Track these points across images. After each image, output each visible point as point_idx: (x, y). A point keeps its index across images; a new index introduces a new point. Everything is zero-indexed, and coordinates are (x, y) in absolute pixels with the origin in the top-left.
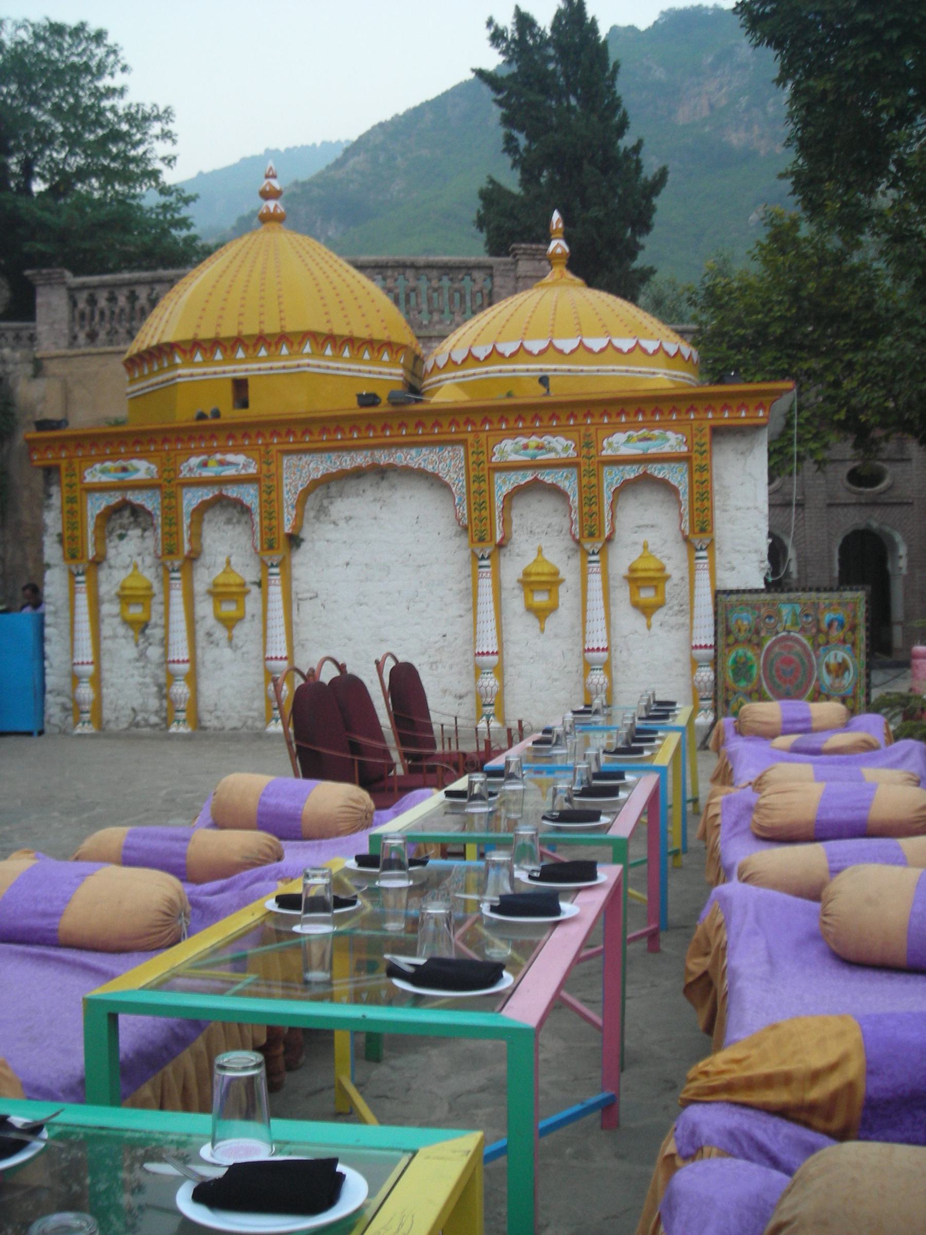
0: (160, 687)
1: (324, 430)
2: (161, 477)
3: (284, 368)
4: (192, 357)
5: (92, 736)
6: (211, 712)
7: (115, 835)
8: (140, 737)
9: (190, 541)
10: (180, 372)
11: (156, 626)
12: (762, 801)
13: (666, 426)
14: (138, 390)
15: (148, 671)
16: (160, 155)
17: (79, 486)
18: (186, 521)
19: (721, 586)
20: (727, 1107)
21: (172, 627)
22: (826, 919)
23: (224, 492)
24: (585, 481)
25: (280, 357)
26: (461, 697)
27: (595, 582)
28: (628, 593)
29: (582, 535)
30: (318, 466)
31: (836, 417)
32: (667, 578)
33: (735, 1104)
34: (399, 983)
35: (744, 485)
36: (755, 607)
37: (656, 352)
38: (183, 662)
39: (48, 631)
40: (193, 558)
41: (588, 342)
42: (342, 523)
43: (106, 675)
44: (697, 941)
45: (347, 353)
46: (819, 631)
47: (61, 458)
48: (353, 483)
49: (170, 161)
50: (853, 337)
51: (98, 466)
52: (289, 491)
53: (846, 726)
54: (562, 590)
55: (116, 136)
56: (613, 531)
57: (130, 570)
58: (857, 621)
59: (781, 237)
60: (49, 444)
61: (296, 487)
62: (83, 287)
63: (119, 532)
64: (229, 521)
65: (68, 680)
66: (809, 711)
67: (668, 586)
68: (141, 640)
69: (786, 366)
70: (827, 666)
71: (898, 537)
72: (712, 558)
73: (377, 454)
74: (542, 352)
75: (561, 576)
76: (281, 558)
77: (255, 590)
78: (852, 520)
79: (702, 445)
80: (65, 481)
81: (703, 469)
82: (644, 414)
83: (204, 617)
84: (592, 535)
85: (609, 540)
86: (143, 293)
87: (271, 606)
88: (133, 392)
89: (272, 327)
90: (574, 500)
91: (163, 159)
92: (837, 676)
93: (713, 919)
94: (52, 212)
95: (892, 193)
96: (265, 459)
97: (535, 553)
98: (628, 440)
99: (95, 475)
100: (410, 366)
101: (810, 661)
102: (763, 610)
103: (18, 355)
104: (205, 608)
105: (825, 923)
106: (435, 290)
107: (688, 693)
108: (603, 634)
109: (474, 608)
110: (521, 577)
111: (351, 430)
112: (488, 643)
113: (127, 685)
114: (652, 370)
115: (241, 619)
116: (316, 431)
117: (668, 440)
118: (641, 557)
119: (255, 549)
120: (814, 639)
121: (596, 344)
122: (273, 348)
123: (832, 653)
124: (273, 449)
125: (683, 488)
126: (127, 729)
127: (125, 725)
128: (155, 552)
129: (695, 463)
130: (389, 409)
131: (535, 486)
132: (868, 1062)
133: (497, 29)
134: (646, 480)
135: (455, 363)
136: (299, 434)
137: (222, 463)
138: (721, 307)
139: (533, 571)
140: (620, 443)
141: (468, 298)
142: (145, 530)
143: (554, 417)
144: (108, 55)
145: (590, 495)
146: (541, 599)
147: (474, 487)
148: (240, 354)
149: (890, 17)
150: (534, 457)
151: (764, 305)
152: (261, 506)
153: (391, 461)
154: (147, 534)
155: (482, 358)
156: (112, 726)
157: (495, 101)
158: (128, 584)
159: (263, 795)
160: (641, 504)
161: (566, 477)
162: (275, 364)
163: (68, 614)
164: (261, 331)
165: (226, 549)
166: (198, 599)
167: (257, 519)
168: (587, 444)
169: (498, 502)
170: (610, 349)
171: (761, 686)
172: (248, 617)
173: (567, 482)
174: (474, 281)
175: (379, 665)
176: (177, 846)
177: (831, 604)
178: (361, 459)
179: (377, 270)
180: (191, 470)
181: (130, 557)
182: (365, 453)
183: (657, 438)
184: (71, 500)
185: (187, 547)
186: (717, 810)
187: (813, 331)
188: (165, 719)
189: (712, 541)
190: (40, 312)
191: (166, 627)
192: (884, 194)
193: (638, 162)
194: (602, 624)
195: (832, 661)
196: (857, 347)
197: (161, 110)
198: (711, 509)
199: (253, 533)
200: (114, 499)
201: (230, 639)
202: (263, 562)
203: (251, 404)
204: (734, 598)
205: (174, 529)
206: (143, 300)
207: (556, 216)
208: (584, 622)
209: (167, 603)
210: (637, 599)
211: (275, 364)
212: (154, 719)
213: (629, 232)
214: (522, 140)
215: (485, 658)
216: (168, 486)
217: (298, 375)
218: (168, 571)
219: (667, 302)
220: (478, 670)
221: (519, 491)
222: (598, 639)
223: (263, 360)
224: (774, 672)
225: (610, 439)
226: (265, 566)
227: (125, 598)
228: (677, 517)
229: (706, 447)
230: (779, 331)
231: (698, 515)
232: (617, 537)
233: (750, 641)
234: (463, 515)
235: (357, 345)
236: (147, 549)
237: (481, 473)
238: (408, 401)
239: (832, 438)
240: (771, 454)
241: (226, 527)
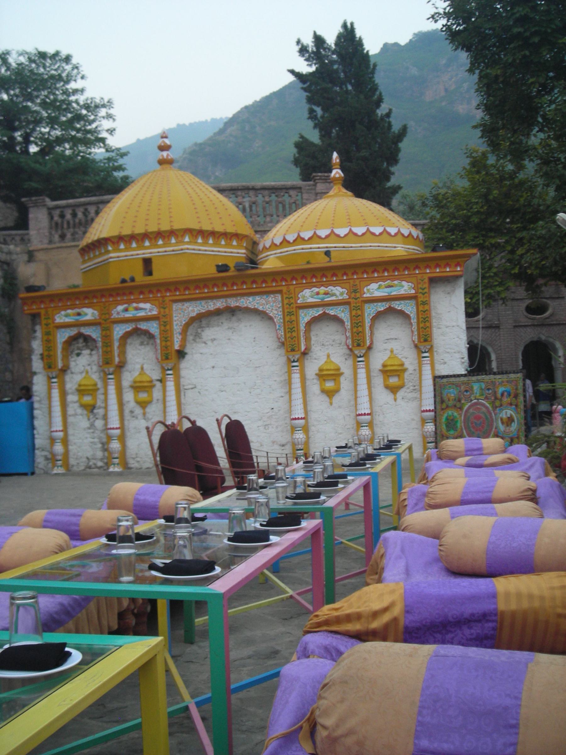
0: (103, 444)
1: (197, 287)
2: (100, 318)
3: (173, 251)
4: (119, 246)
5: (63, 475)
6: (134, 458)
7: (40, 514)
8: (92, 475)
9: (119, 356)
10: (112, 255)
11: (100, 408)
12: (431, 490)
13: (401, 278)
14: (88, 267)
15: (95, 435)
16: (106, 128)
17: (52, 326)
18: (116, 344)
19: (438, 373)
20: (326, 634)
21: (110, 408)
22: (441, 548)
23: (139, 326)
24: (354, 313)
25: (170, 245)
26: (283, 446)
27: (362, 373)
28: (382, 380)
29: (353, 346)
31: (513, 272)
32: (405, 370)
33: (332, 632)
34: (154, 573)
35: (450, 313)
36: (458, 386)
37: (396, 234)
38: (117, 428)
39: (36, 412)
40: (121, 366)
41: (355, 230)
42: (209, 343)
43: (71, 438)
44: (372, 565)
45: (211, 241)
46: (496, 398)
47: (41, 308)
48: (216, 318)
49: (112, 131)
50: (522, 223)
51: (63, 313)
52: (177, 324)
53: (504, 452)
54: (342, 379)
55: (78, 117)
56: (372, 343)
57: (84, 375)
58: (518, 392)
59: (477, 164)
60: (34, 300)
61: (181, 322)
62: (57, 207)
63: (77, 352)
64: (142, 344)
65: (48, 441)
66: (481, 444)
67: (406, 375)
68: (91, 416)
69: (481, 242)
70: (502, 419)
71: (558, 345)
73: (229, 300)
74: (327, 237)
75: (342, 371)
76: (173, 365)
77: (158, 384)
78: (529, 335)
79: (423, 289)
80: (44, 322)
82: (388, 271)
83: (128, 402)
85: (370, 348)
86: (92, 209)
87: (168, 394)
88: (84, 268)
89: (165, 227)
90: (348, 324)
91: (107, 131)
92: (508, 426)
93: (379, 551)
94: (40, 164)
95: (541, 135)
96: (162, 306)
97: (326, 357)
98: (379, 288)
99: (61, 318)
100: (250, 248)
101: (491, 417)
102: (462, 387)
103: (18, 249)
104: (129, 396)
105: (440, 550)
106: (267, 203)
107: (420, 439)
108: (367, 405)
109: (290, 393)
110: (317, 372)
111: (213, 287)
112: (299, 412)
113: (84, 444)
114: (394, 245)
115: (149, 402)
116: (192, 287)
117: (403, 286)
118: (389, 358)
119: (158, 359)
120: (493, 403)
121: (360, 230)
122: (166, 239)
123: (504, 411)
124: (167, 299)
125: (413, 315)
126: (84, 470)
127: (83, 468)
128: (98, 363)
129: (420, 300)
130: (236, 273)
132: (406, 606)
133: (303, 46)
134: (391, 311)
135: (276, 245)
136: (182, 289)
137: (137, 309)
138: (442, 207)
139: (325, 368)
140: (374, 289)
141: (287, 206)
142: (92, 350)
143: (334, 275)
144: (73, 69)
145: (357, 321)
146: (330, 385)
147: (287, 319)
148: (147, 243)
149: (533, 30)
150: (322, 300)
151: (467, 205)
152: (160, 334)
153: (237, 305)
154: (94, 352)
155: (291, 241)
156: (75, 469)
157: (302, 88)
158: (83, 383)
159: (137, 494)
160: (389, 326)
161: (343, 311)
162: (168, 249)
163: (47, 402)
164: (159, 229)
165: (141, 360)
166: (124, 391)
167: (158, 341)
168: (355, 290)
169: (302, 327)
170: (368, 233)
171: (463, 432)
172: (155, 401)
173: (343, 313)
174: (290, 196)
175: (219, 422)
176: (74, 519)
177: (503, 382)
178: (219, 304)
179: (232, 192)
180: (118, 313)
181: (84, 366)
182: (221, 300)
183: (396, 286)
184: (48, 334)
185: (117, 360)
186: (405, 497)
187: (498, 220)
188: (107, 464)
189: (432, 346)
190: (32, 224)
191: (106, 408)
192: (535, 136)
193: (389, 123)
194: (366, 399)
195: (504, 416)
196: (524, 228)
197: (106, 100)
198: (430, 327)
199: (157, 350)
201: (144, 414)
202: (163, 368)
203: (154, 273)
204: (445, 380)
205: (109, 349)
206: (92, 214)
207: (335, 155)
208: (356, 398)
209: (106, 394)
210: (388, 383)
211: (168, 249)
212: (100, 464)
213: (385, 164)
214: (319, 111)
215: (297, 421)
216: (105, 323)
217: (181, 255)
218: (106, 374)
219: (417, 208)
220: (293, 429)
222: (364, 408)
223: (160, 246)
224: (470, 424)
225: (369, 287)
226: (164, 370)
227: (81, 391)
228: (410, 333)
229: (426, 290)
230: (476, 220)
231: (423, 332)
232: (374, 346)
233: (455, 406)
234: (281, 335)
235: (217, 236)
236: (93, 361)
237: (292, 310)
238: (247, 268)
239: (511, 284)
241: (140, 347)
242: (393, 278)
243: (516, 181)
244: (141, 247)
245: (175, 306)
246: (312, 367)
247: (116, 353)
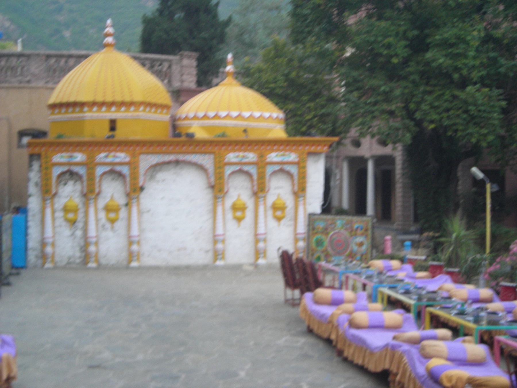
1: (158, 146)
13: (291, 151)
18: (97, 180)
30: (154, 159)
40: (99, 194)
60: (37, 145)
64: (113, 179)
72: (304, 200)
81: (304, 167)
84: (259, 191)
89: (128, 99)
90: (255, 177)
96: (133, 155)
98: (277, 156)
131: (240, 171)
140: (274, 157)
146: (239, 214)
147: (218, 171)
150: (241, 160)
165: (112, 191)
168: (262, 156)
173: (253, 170)
181: (69, 193)
196: (310, 100)
200: (65, 168)
201: (112, 228)
216: (90, 165)
221: (234, 173)
222: (261, 230)
227: (66, 209)
237: (220, 165)
240: (326, 162)
242: (286, 151)
243: (304, 63)
244: (108, 110)
245: (142, 157)
246: (229, 202)
247: (97, 185)
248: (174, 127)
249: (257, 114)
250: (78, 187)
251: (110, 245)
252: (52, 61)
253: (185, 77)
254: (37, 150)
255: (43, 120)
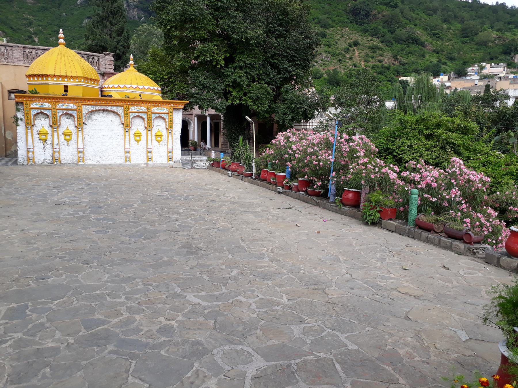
8: (47, 166)
13: (163, 107)
30: (90, 108)
43: (35, 151)
64: (68, 118)
80: (25, 106)
84: (149, 127)
90: (146, 120)
99: (33, 105)
124: (80, 104)
134: (160, 117)
140: (155, 109)
145: (149, 120)
148: (66, 80)
165: (67, 124)
167: (76, 119)
178: (100, 108)
181: (42, 124)
200: (39, 111)
201: (68, 145)
207: (131, 55)
212: (49, 161)
221: (135, 117)
222: (149, 147)
237: (127, 113)
246: (132, 132)
247: (58, 121)
248: (101, 92)
249: (147, 87)
250: (47, 121)
251: (68, 154)
252: (27, 51)
253: (107, 66)
254: (20, 100)
255: (24, 85)
